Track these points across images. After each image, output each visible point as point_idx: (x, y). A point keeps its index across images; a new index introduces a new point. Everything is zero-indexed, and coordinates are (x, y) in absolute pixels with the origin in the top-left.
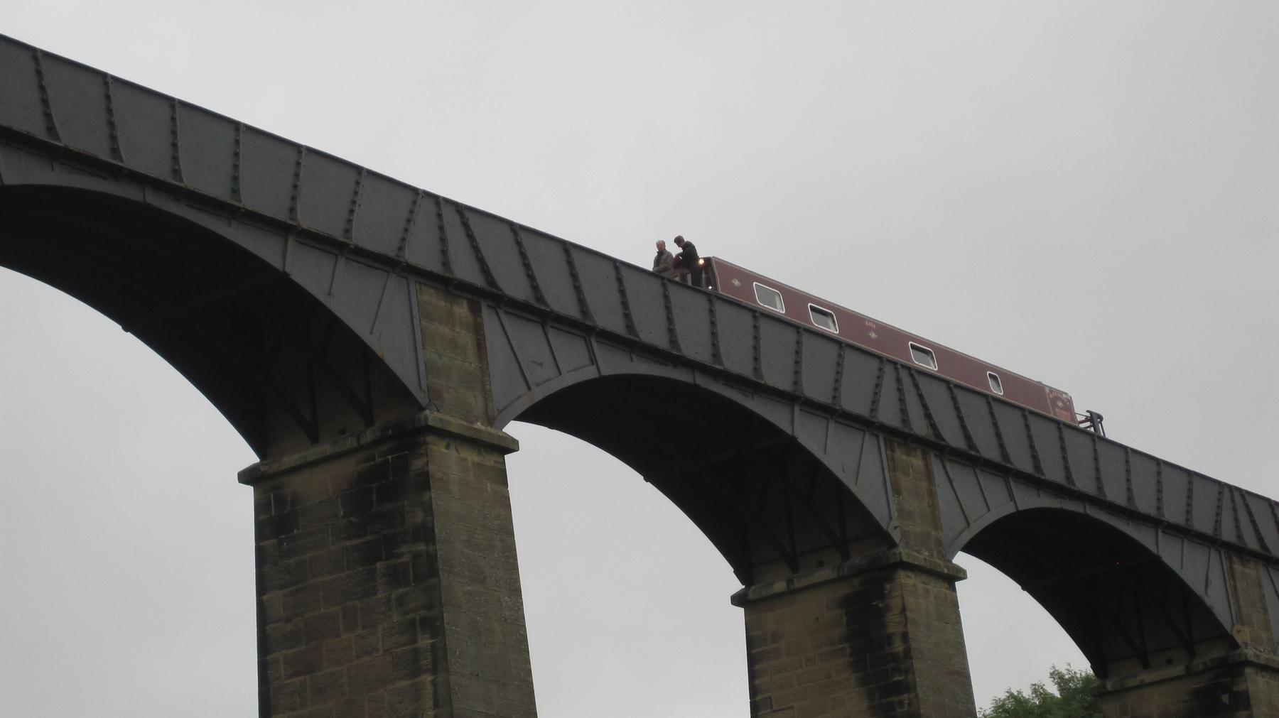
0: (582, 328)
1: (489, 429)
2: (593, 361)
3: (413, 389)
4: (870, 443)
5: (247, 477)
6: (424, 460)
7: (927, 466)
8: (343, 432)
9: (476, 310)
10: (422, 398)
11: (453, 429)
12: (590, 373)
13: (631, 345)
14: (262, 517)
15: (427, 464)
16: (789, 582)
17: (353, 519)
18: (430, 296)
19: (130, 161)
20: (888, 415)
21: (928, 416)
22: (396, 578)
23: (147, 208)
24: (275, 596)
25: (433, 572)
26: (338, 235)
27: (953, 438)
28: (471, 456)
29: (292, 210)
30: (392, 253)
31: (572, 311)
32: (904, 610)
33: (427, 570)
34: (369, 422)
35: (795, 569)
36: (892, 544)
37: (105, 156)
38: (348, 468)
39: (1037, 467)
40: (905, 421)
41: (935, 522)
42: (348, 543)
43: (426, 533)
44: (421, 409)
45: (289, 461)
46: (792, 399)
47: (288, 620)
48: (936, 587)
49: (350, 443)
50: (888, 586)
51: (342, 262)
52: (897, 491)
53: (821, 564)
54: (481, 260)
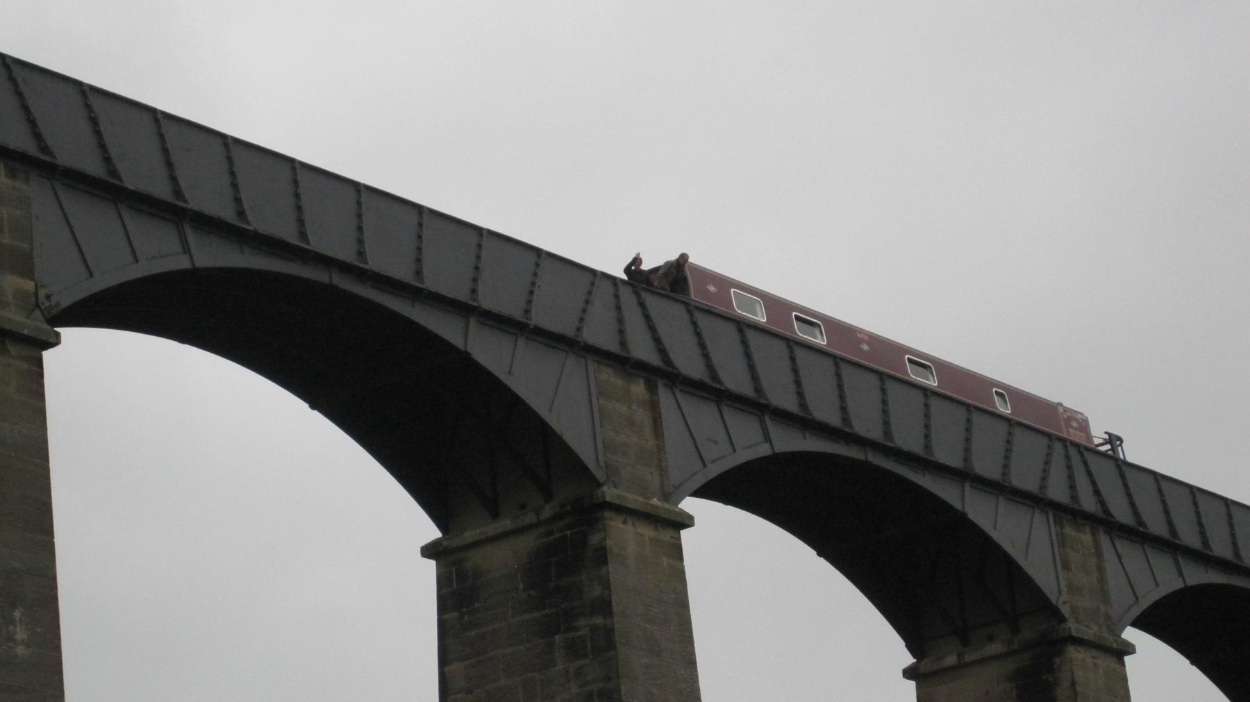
0: (757, 406)
1: (667, 506)
2: (768, 439)
3: (592, 466)
4: (1039, 520)
5: (429, 551)
6: (602, 534)
7: (1097, 544)
8: (523, 507)
9: (652, 388)
10: (600, 475)
11: (632, 506)
12: (764, 450)
13: (804, 422)
14: (444, 591)
15: (605, 539)
16: (960, 656)
17: (532, 593)
18: (608, 376)
19: (316, 244)
20: (1058, 492)
21: (1097, 492)
22: (574, 650)
23: (333, 290)
24: (456, 667)
25: (610, 645)
26: (518, 314)
27: (1122, 514)
28: (647, 531)
29: (474, 291)
30: (569, 332)
31: (747, 390)
32: (1073, 684)
33: (605, 643)
34: (548, 497)
35: (965, 642)
36: (1062, 619)
37: (294, 241)
38: (526, 544)
39: (1205, 543)
40: (1074, 498)
41: (1105, 599)
42: (527, 616)
43: (604, 606)
44: (599, 485)
45: (470, 535)
46: (963, 475)
47: (469, 691)
48: (1106, 662)
49: (530, 518)
50: (1057, 660)
51: (521, 342)
52: (1066, 566)
53: (991, 639)
54: (657, 340)
